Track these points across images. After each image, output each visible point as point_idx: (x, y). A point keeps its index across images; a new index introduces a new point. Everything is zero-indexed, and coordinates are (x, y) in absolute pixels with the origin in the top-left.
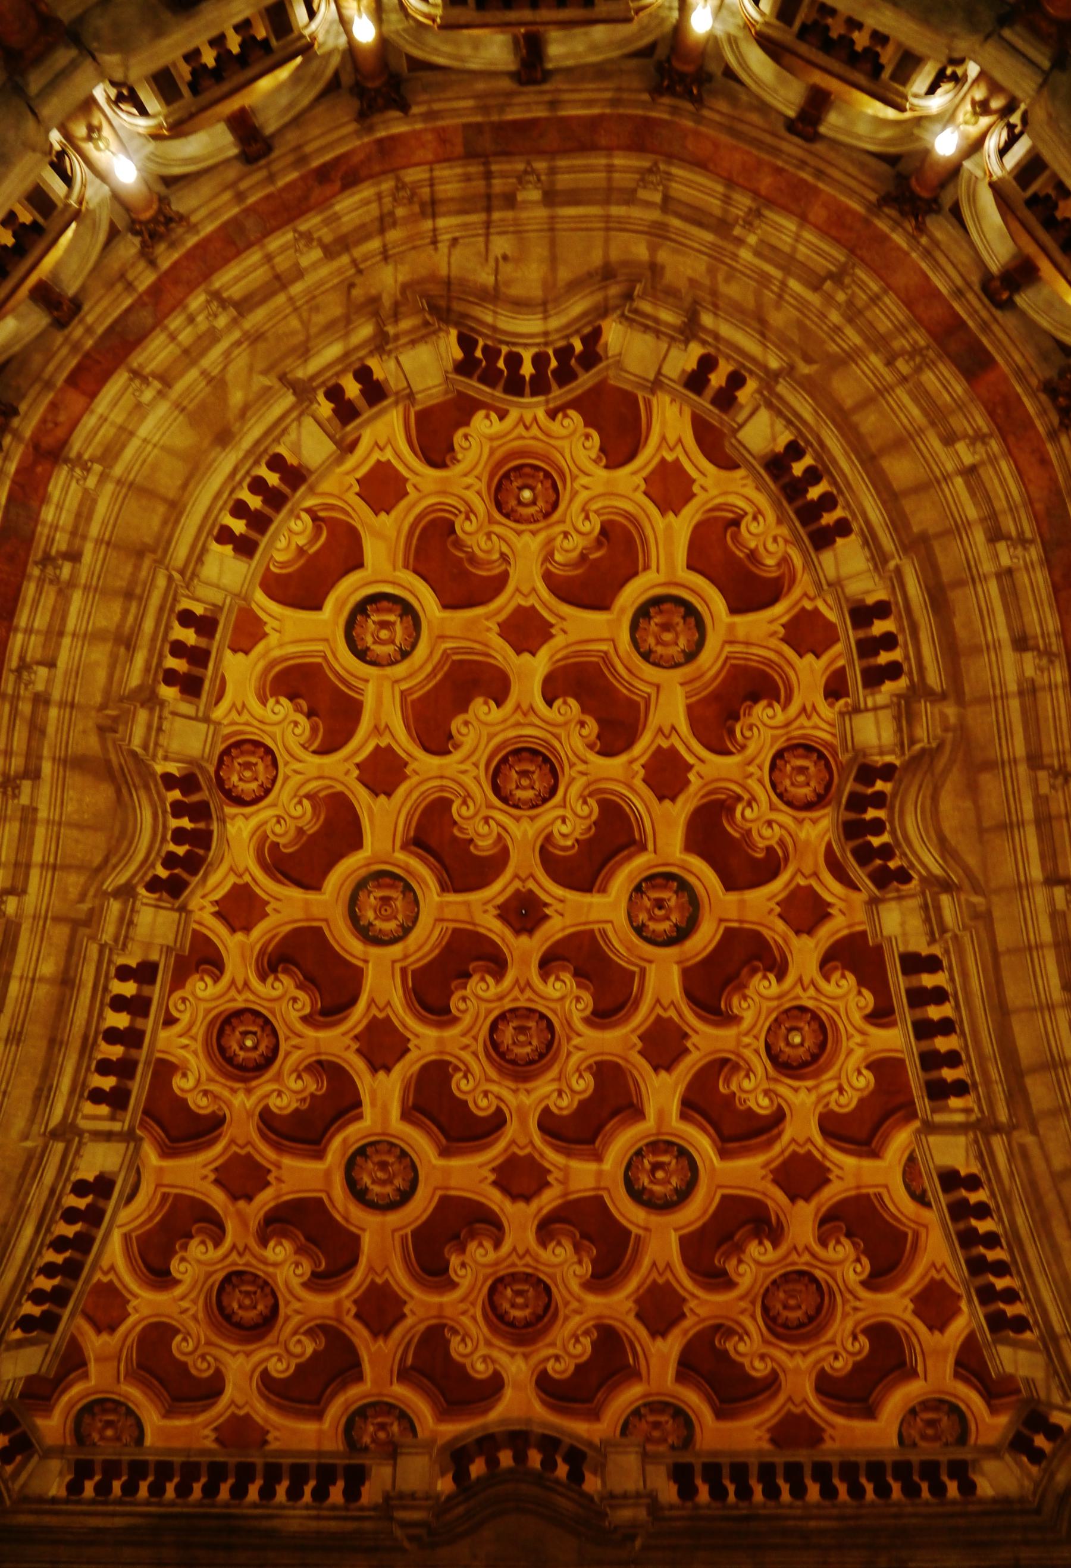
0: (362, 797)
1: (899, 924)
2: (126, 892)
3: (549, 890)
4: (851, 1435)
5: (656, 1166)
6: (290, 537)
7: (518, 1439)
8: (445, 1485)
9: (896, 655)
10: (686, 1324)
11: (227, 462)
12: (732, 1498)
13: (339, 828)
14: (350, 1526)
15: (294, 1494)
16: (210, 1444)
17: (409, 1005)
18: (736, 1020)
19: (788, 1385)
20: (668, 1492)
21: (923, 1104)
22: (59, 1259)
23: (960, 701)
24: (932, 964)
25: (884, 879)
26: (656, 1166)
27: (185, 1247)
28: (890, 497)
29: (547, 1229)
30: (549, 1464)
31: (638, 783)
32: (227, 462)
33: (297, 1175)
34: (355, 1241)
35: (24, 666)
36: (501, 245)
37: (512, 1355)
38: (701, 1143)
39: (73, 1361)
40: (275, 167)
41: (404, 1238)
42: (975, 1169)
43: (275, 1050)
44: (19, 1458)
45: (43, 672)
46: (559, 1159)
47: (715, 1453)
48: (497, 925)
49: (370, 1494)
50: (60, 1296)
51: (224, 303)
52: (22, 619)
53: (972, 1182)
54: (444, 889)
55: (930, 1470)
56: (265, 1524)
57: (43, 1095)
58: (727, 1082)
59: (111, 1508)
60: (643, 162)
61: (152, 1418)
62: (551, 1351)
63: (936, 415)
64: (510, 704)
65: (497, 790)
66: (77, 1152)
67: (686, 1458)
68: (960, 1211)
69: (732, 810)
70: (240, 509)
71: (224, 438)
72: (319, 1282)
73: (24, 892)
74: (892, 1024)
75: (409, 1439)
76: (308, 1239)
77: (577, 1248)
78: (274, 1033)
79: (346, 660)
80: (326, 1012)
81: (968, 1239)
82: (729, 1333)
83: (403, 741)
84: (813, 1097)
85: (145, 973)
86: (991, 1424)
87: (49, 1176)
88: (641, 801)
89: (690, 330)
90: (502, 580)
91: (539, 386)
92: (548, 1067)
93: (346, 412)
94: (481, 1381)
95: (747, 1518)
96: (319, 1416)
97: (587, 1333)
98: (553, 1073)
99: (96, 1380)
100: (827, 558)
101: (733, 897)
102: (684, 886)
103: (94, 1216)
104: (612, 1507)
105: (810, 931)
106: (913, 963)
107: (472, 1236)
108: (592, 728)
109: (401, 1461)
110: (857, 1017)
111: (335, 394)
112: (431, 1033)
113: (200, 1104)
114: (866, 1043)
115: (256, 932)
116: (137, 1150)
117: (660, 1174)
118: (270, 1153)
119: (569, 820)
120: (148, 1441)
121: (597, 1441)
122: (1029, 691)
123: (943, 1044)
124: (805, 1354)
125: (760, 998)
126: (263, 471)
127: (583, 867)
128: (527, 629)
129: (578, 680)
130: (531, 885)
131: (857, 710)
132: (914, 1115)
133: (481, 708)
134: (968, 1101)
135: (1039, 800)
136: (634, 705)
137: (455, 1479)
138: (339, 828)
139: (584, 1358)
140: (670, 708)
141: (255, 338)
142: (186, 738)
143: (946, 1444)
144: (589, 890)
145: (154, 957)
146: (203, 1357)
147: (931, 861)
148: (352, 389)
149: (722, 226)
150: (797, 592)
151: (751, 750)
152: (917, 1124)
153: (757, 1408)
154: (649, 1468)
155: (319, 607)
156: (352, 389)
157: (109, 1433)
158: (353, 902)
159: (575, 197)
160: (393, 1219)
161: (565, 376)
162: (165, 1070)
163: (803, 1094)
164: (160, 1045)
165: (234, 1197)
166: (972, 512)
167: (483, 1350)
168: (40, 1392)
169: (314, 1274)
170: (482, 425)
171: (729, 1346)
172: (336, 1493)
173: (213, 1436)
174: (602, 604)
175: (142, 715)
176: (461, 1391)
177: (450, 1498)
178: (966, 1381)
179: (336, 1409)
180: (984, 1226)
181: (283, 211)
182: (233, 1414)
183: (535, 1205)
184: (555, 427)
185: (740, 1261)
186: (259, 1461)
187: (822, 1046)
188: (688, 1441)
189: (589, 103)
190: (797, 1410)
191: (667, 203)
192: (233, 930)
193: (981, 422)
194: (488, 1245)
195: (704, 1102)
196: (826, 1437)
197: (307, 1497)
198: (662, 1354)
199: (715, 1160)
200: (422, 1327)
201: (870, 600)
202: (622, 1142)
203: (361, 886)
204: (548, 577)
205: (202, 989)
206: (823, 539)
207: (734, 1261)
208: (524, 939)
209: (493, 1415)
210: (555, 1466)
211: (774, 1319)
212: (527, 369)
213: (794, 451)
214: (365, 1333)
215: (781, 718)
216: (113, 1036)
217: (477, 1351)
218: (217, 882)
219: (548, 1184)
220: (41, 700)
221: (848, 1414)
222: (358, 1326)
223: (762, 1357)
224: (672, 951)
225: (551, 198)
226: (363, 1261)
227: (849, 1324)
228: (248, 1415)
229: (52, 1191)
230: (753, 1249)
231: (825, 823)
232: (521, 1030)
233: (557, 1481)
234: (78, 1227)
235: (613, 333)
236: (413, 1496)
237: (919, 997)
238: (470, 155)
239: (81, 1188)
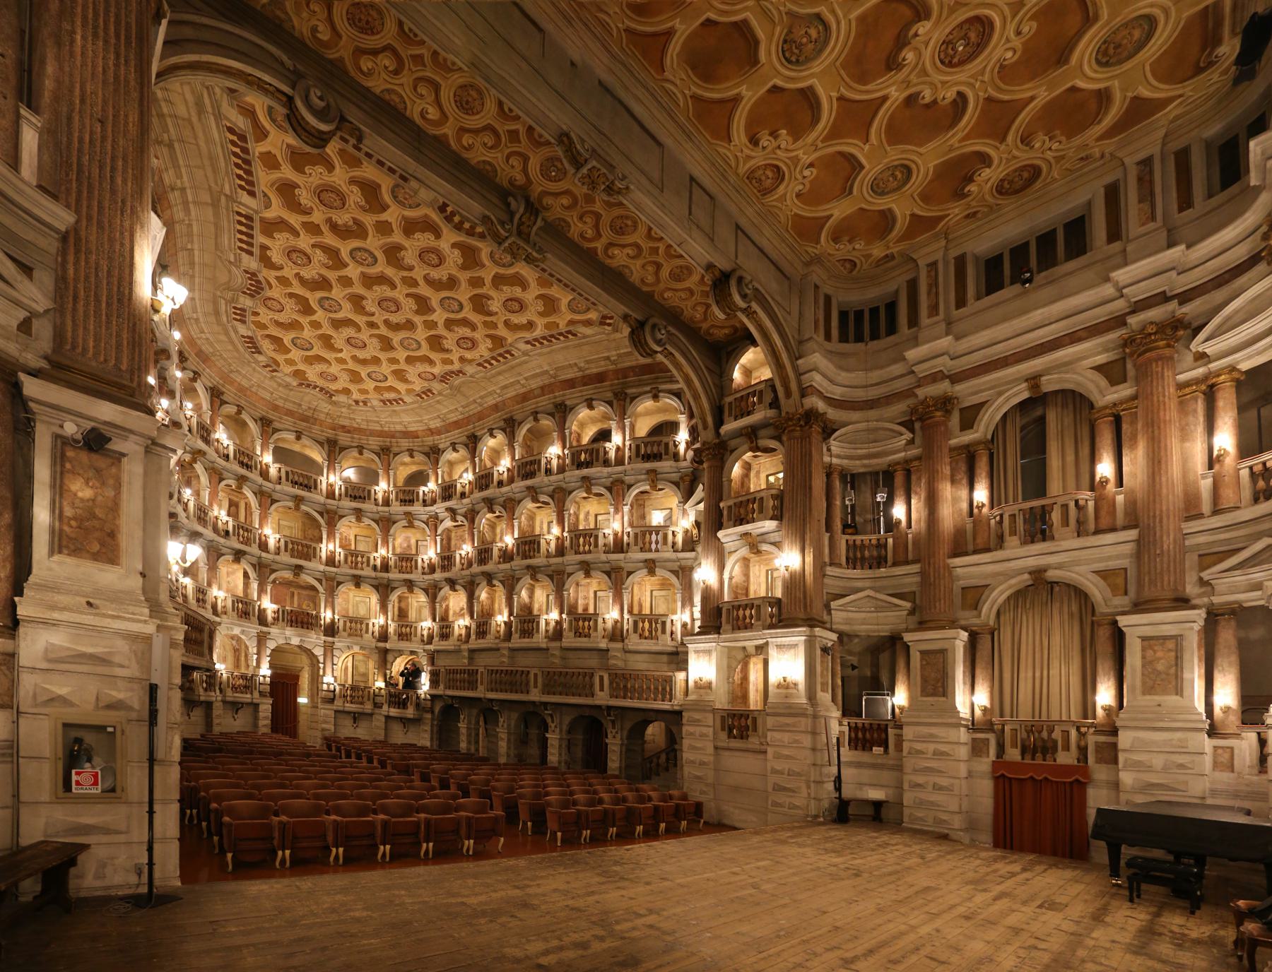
1: (252, 263)
6: (392, 395)
7: (458, 227)
11: (398, 408)
13: (409, 360)
23: (214, 295)
24: (240, 248)
28: (227, 334)
29: (411, 269)
33: (475, 318)
39: (571, 322)
50: (561, 334)
63: (211, 344)
72: (489, 298)
79: (390, 378)
83: (384, 363)
85: (479, 365)
88: (325, 324)
91: (315, 387)
93: (365, 403)
99: (570, 316)
100: (250, 334)
103: (536, 340)
106: (250, 253)
113: (489, 341)
128: (341, 361)
135: (193, 269)
142: (436, 386)
149: (259, 386)
153: (364, 178)
168: (588, 323)
179: (511, 271)
188: (397, 186)
193: (199, 342)
198: (393, 215)
205: (468, 355)
206: (251, 338)
217: (454, 257)
218: (449, 367)
220: (464, 407)
227: (311, 179)
230: (340, 222)
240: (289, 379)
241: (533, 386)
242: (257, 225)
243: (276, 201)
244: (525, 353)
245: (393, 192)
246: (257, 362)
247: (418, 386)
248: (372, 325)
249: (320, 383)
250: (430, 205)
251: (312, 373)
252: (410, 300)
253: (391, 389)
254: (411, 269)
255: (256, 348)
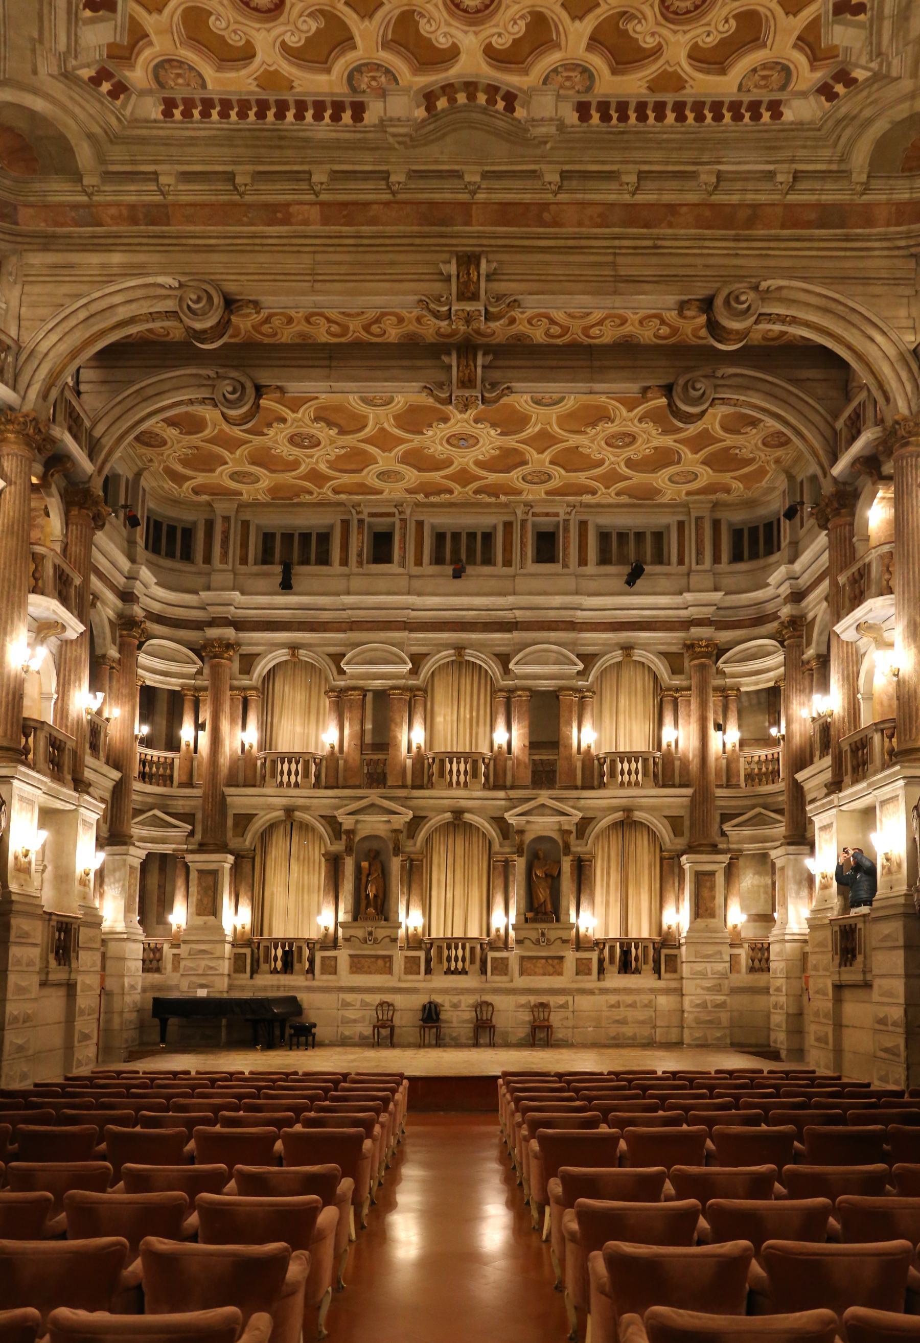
4: (705, 85)
7: (471, 87)
8: (420, 113)
10: (598, 11)
12: (614, 121)
14: (359, 136)
15: (318, 117)
16: (253, 88)
19: (667, 55)
20: (572, 117)
30: (491, 101)
37: (466, 32)
44: (122, 96)
47: (607, 96)
49: (370, 117)
55: (754, 107)
56: (301, 134)
59: (195, 125)
61: (208, 72)
62: (495, 30)
67: (584, 98)
75: (393, 86)
82: (633, 17)
86: (808, 77)
94: (444, 50)
95: (623, 133)
96: (328, 71)
97: (523, 17)
104: (533, 126)
109: (388, 99)
120: (210, 86)
121: (525, 88)
124: (685, 32)
137: (428, 109)
139: (521, 34)
143: (771, 90)
146: (235, 32)
154: (559, 104)
157: (180, 81)
167: (444, 29)
171: (630, 27)
172: (347, 117)
173: (255, 83)
176: (430, 57)
177: (423, 121)
178: (801, 49)
182: (266, 71)
186: (291, 99)
188: (589, 89)
190: (670, 70)
196: (687, 86)
197: (327, 119)
200: (397, 12)
209: (453, 72)
210: (496, 102)
211: (667, 8)
214: (355, 16)
221: (708, 72)
222: (347, 10)
223: (653, 34)
227: (725, 12)
228: (276, 71)
233: (497, 112)
236: (399, 120)
245: (591, 77)
250: (529, 93)
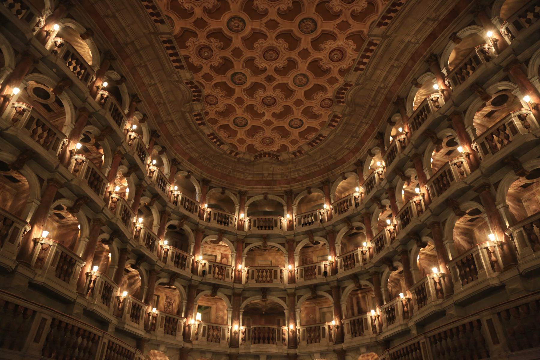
0: (303, 99)
1: (186, 75)
2: (357, 84)
3: (264, 83)
5: (238, 27)
6: (312, 136)
9: (195, 118)
13: (308, 95)
17: (297, 62)
18: (221, 58)
21: (173, 39)
22: (397, 7)
24: (177, 67)
25: (191, 83)
26: (238, 27)
27: (362, 10)
29: (266, 12)
31: (245, 100)
32: (321, 146)
34: (316, 11)
35: (367, 123)
36: (271, 169)
38: (226, 31)
40: (305, 185)
41: (304, 11)
42: (156, 24)
43: (330, 54)
45: (363, 121)
46: (262, 29)
48: (276, 77)
51: (318, 165)
52: (364, 131)
53: (156, 21)
54: (287, 84)
57: (389, 45)
58: (221, 45)
60: (247, 179)
64: (272, 112)
65: (275, 99)
66: (384, 32)
68: (158, 14)
69: (226, 95)
70: (321, 140)
71: (321, 149)
73: (379, 87)
74: (184, 56)
76: (329, 11)
77: (258, 8)
78: (329, 57)
79: (304, 120)
80: (317, 61)
81: (154, 7)
83: (294, 108)
84: (200, 41)
85: (357, 69)
87: (393, 26)
88: (245, 97)
89: (239, 159)
90: (272, 130)
91: (265, 154)
92: (264, 50)
93: (300, 152)
98: (264, 48)
100: (211, 131)
101: (224, 81)
102: (235, 83)
103: (384, 18)
105: (206, 74)
106: (182, 67)
107: (285, 11)
108: (255, 109)
110: (192, 57)
111: (301, 153)
112: (293, 56)
113: (351, 42)
114: (190, 50)
115: (330, 76)
116: (369, 33)
117: (237, 25)
118: (335, 31)
119: (260, 94)
122: (169, 114)
123: (171, 51)
125: (216, 61)
126: (315, 145)
127: (255, 87)
128: (268, 123)
129: (257, 115)
130: (268, 84)
131: (202, 110)
132: (174, 36)
133: (278, 112)
134: (162, 39)
136: (247, 111)
138: (308, 95)
140: (239, 111)
141: (314, 160)
142: (338, 109)
144: (255, 83)
145: (354, 72)
147: (182, 86)
148: (298, 154)
150: (216, 127)
151: (222, 105)
152: (174, 34)
155: (308, 127)
156: (298, 154)
158: (307, 82)
159: (259, 174)
160: (306, 16)
161: (261, 155)
162: (357, 50)
163: (203, 41)
164: (357, 55)
165: (347, 22)
166: (186, 138)
169: (329, 2)
170: (276, 149)
174: (253, 126)
175: (346, 112)
180: (150, 10)
181: (307, 177)
183: (269, 19)
184: (262, 149)
185: (214, 3)
187: (199, 52)
189: (256, 188)
191: (244, 173)
192: (335, 77)
194: (281, 9)
195: (228, 41)
199: (223, 28)
201: (202, 126)
202: (247, 31)
203: (305, 85)
204: (264, 130)
205: (344, 65)
206: (212, 134)
207: (215, 3)
208: (270, 74)
212: (267, 155)
213: (219, 145)
215: (217, 109)
216: (368, 57)
218: (337, 86)
219: (265, 23)
220: (365, 117)
224: (236, 71)
225: (263, 174)
226: (315, 5)
229: (393, 24)
230: (211, 6)
231: (205, 92)
232: (271, 57)
234: (389, 15)
235: (253, 159)
237: (179, 61)
238: (276, 181)
239: (386, 24)
240: (247, 157)
241: (405, 62)
242: (175, 44)
243: (174, 16)
244: (384, 36)
246: (225, 153)
247: (325, 115)
248: (270, 79)
249: (267, 149)
251: (256, 141)
252: (281, 41)
253: (310, 130)
254: (266, 12)
255: (219, 140)
